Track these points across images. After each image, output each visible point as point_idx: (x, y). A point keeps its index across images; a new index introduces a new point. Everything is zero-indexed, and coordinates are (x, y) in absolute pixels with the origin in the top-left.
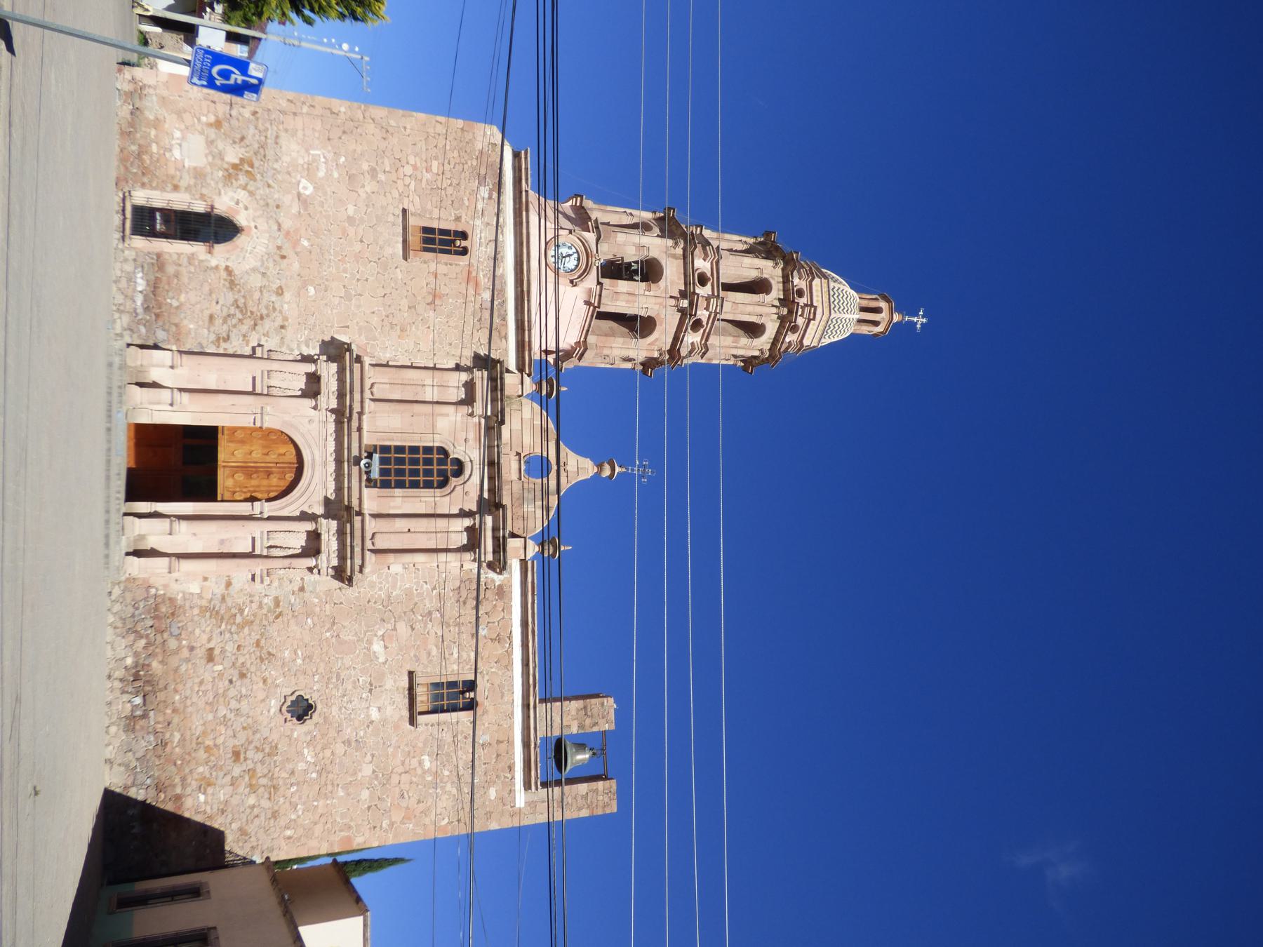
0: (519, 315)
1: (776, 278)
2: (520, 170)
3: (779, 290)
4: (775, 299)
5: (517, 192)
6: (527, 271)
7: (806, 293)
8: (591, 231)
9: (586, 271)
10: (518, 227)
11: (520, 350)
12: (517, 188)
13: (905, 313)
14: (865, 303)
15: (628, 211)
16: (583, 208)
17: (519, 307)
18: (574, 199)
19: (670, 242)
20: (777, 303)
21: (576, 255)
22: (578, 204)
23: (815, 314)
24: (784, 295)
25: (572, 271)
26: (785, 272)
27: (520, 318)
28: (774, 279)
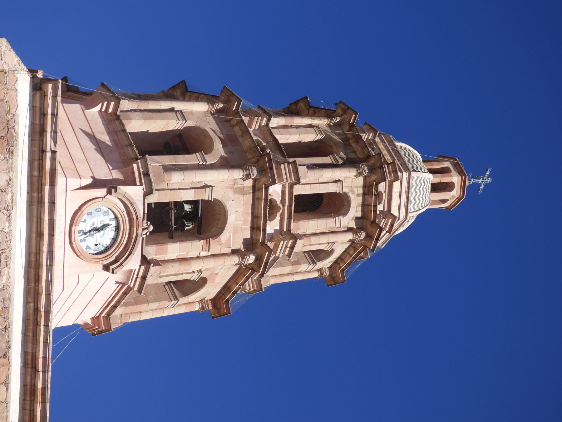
0: (30, 345)
1: (355, 190)
2: (44, 115)
3: (358, 205)
4: (352, 219)
5: (36, 149)
6: (47, 281)
7: (385, 197)
8: (138, 183)
9: (127, 251)
10: (35, 208)
11: (28, 398)
12: (37, 143)
13: (471, 175)
14: (438, 179)
15: (178, 105)
16: (118, 118)
17: (30, 334)
18: (106, 103)
19: (238, 174)
20: (353, 225)
21: (114, 223)
22: (110, 111)
23: (392, 225)
24: (363, 211)
25: (107, 249)
26: (368, 180)
27: (30, 350)
28: (353, 192)
